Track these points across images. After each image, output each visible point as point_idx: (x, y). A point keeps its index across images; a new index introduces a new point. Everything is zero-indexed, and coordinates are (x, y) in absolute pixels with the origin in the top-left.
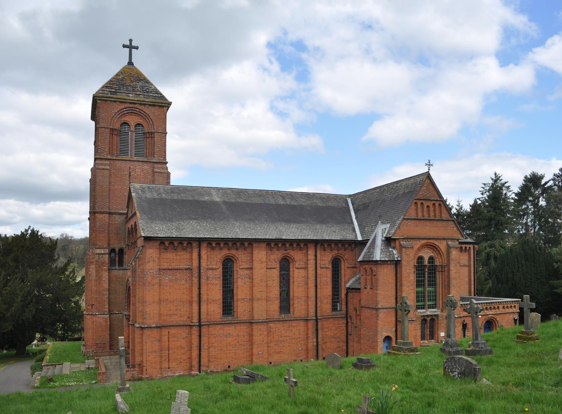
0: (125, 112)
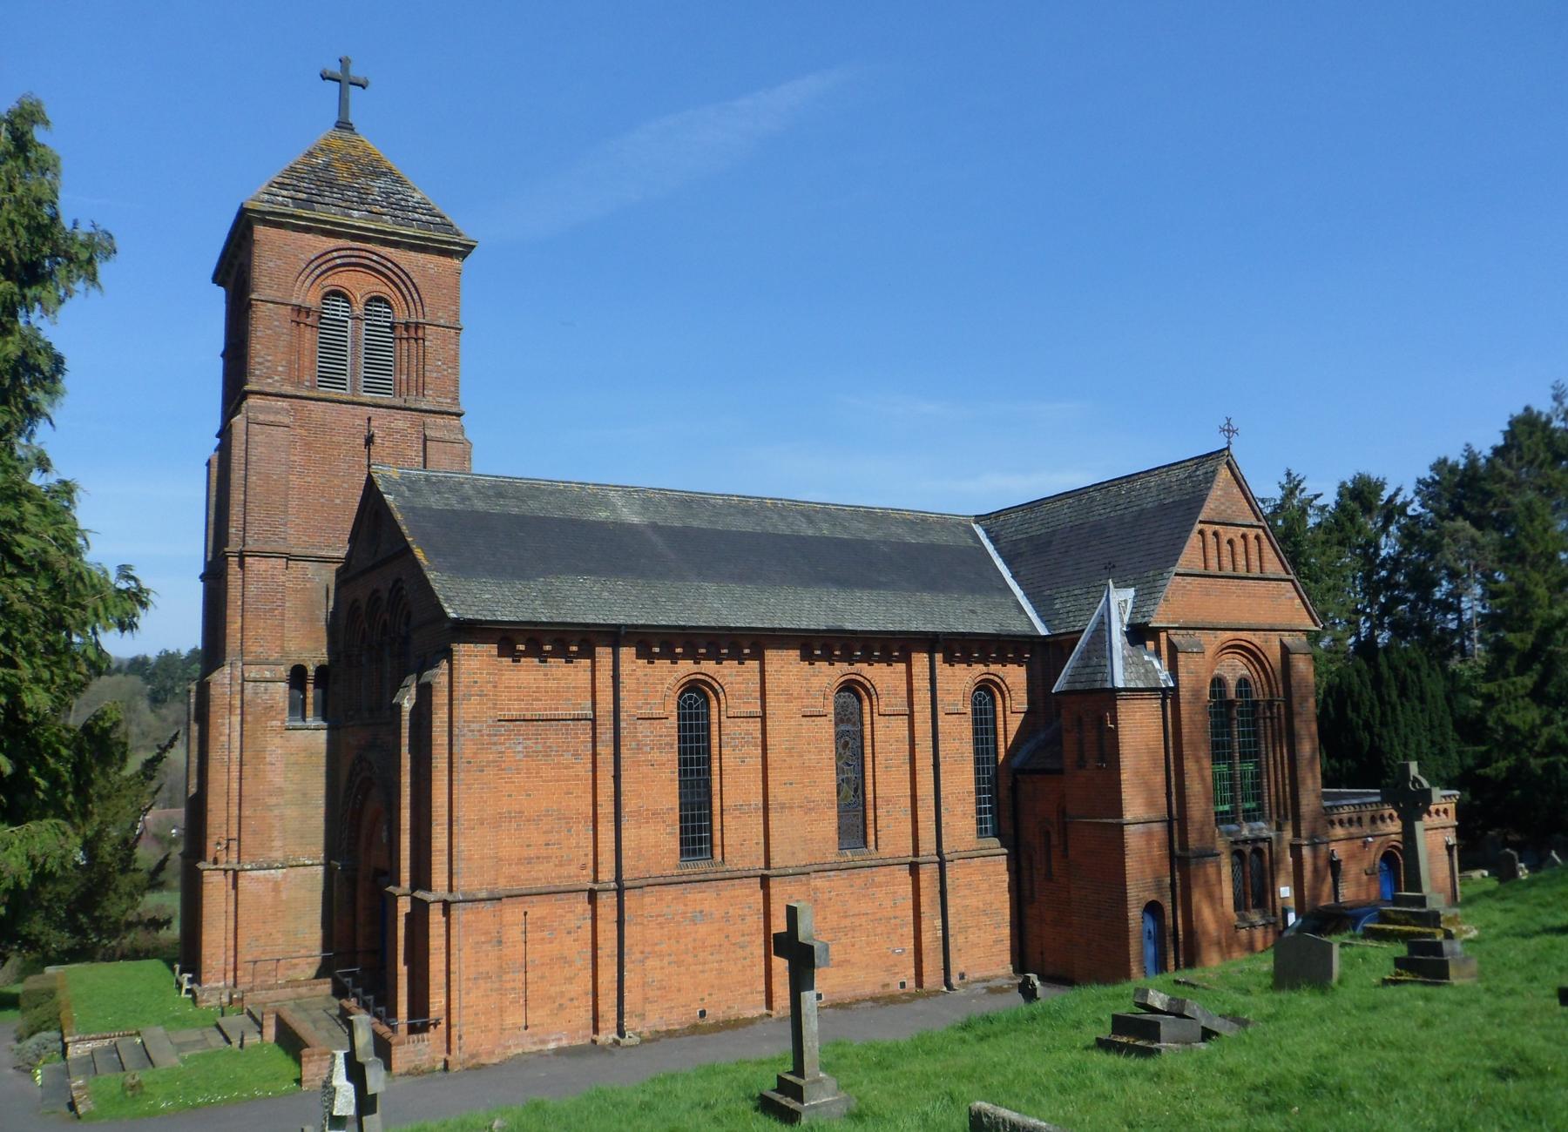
0: (338, 261)
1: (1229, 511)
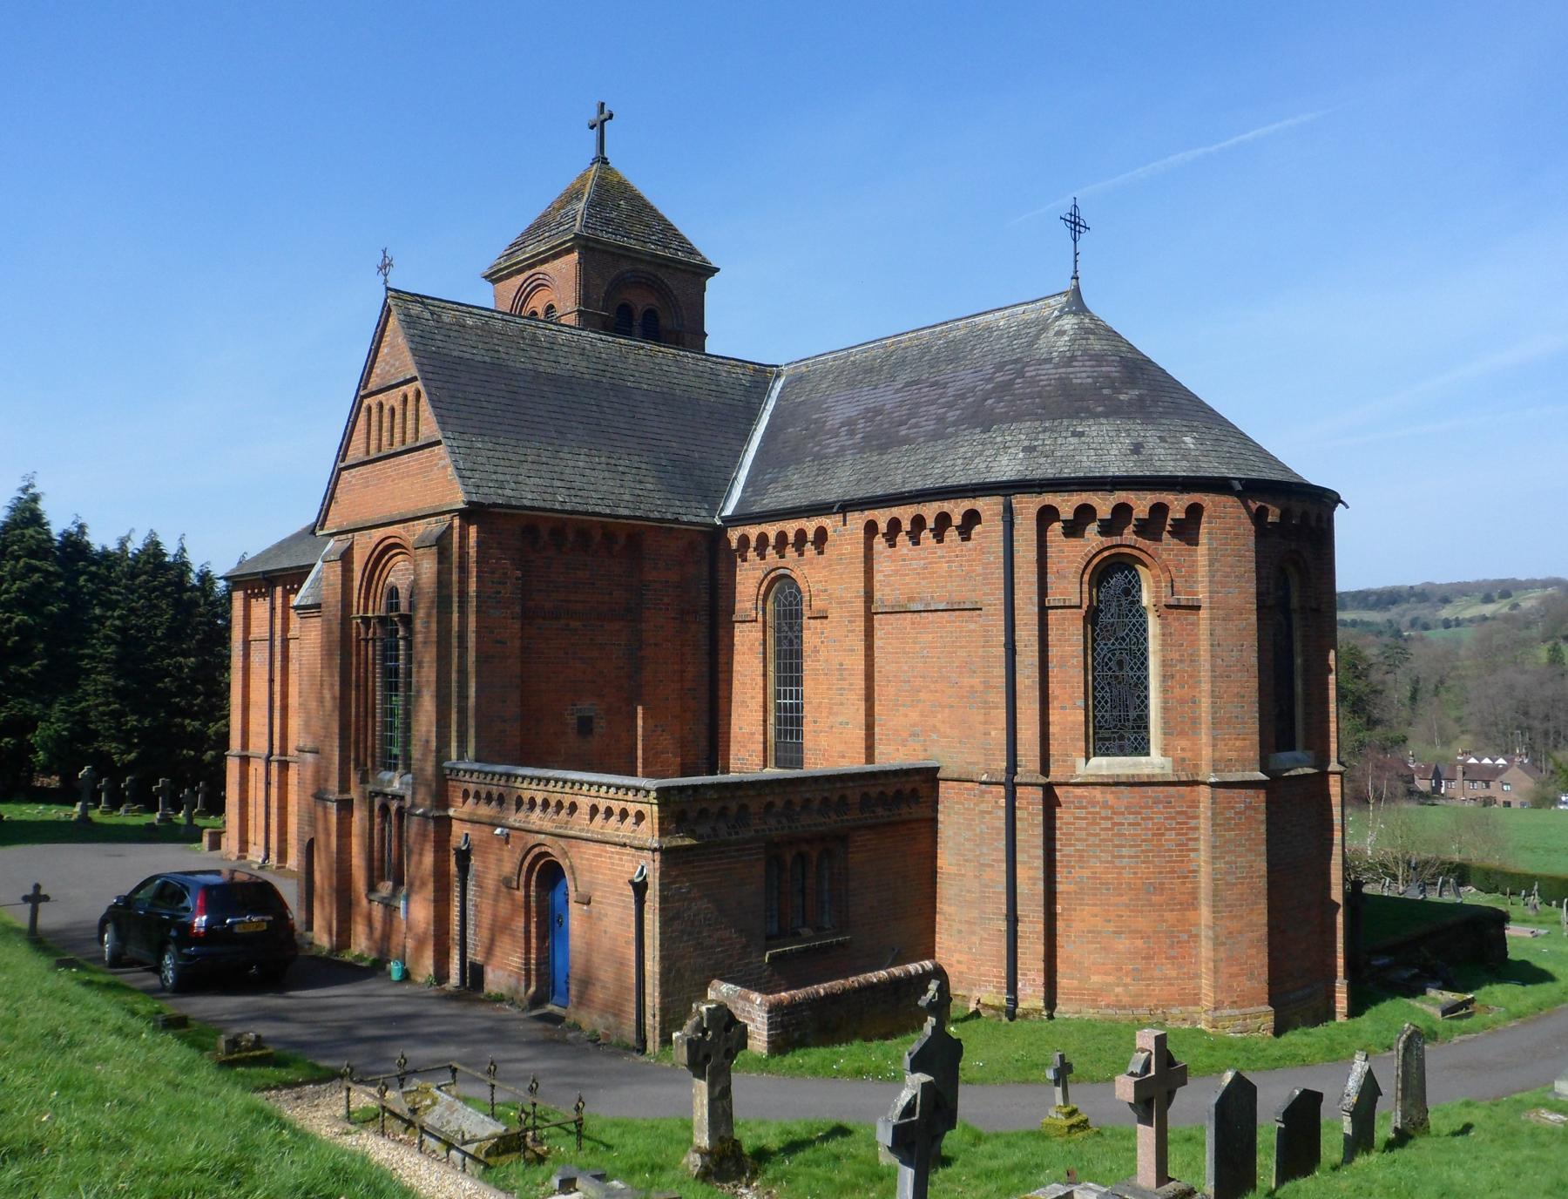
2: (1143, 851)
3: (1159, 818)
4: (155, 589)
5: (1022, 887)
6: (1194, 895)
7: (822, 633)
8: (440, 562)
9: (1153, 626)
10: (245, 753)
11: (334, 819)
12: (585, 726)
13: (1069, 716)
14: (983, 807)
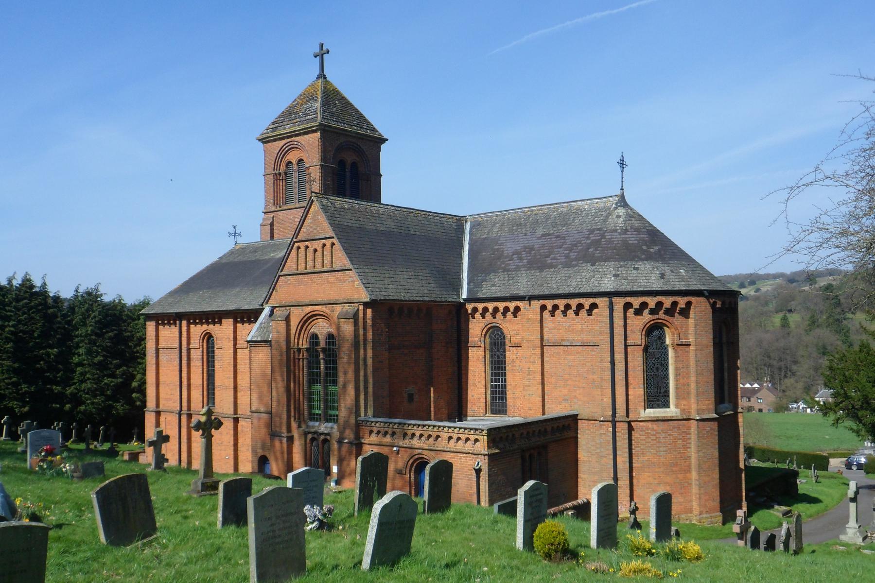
0: (287, 149)
1: (315, 231)
2: (669, 449)
3: (675, 435)
4: (32, 308)
5: (619, 466)
6: (689, 466)
7: (517, 353)
8: (355, 326)
9: (671, 353)
10: (158, 410)
11: (285, 446)
12: (411, 397)
13: (638, 391)
14: (602, 431)
